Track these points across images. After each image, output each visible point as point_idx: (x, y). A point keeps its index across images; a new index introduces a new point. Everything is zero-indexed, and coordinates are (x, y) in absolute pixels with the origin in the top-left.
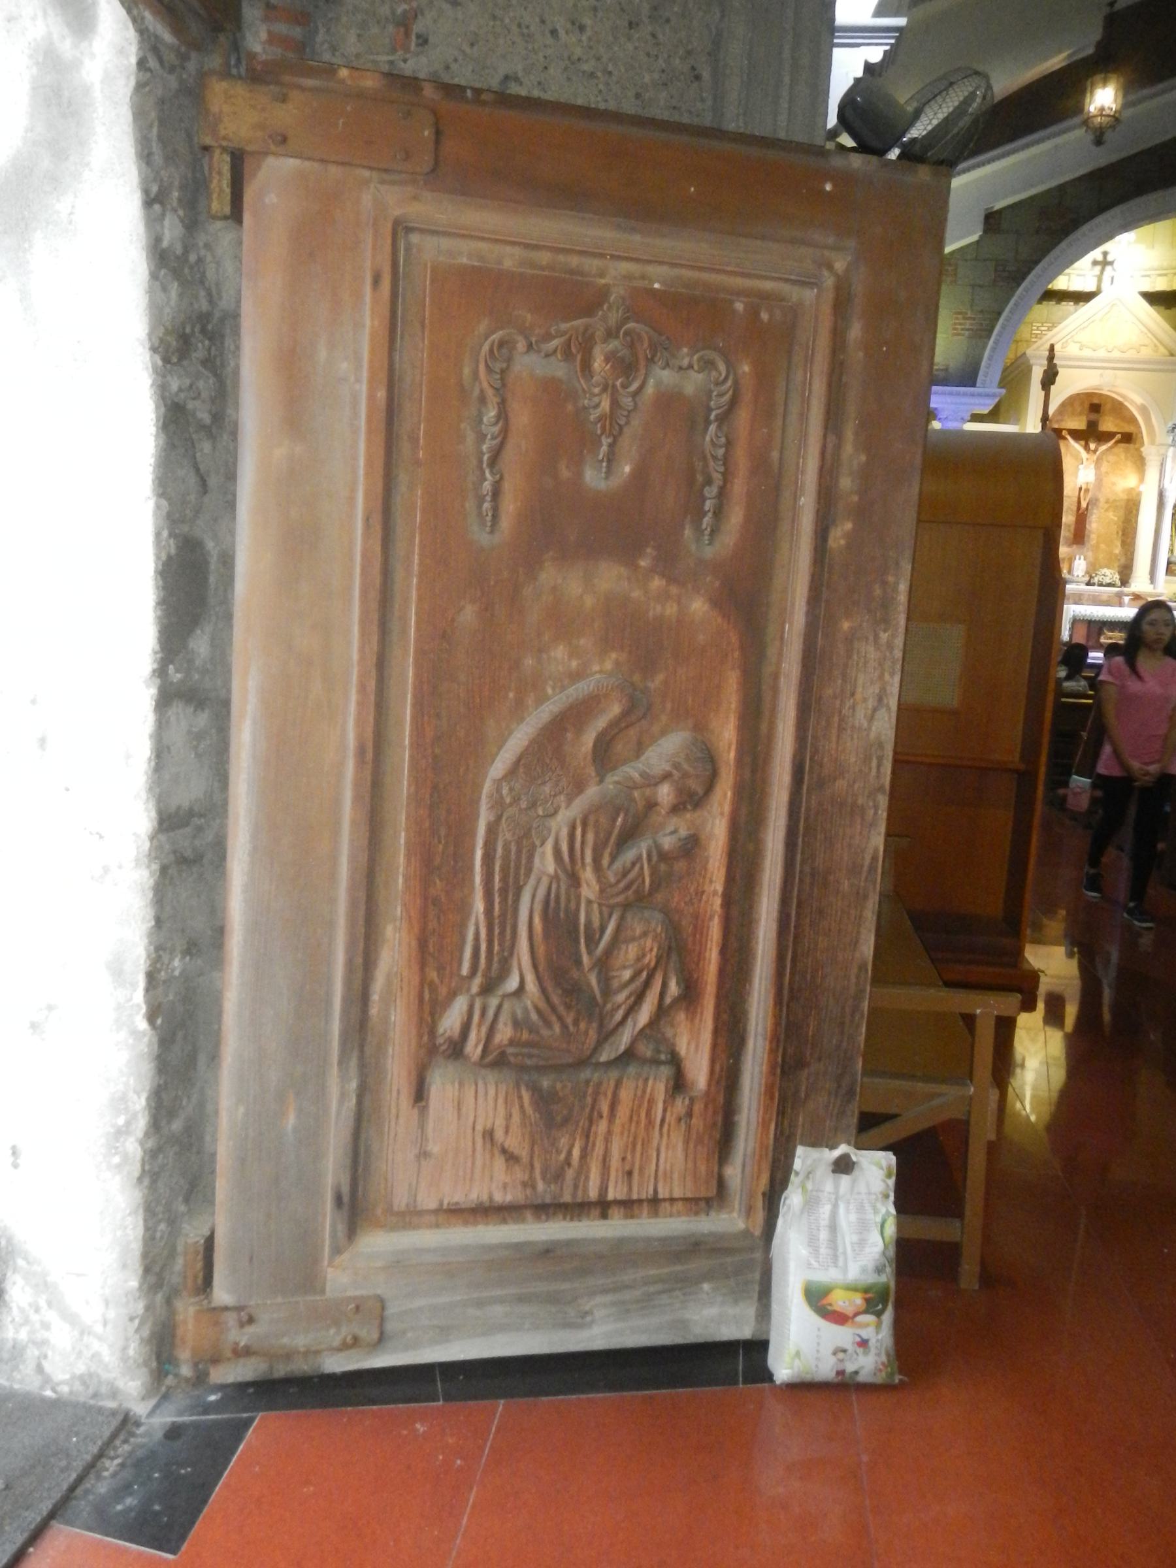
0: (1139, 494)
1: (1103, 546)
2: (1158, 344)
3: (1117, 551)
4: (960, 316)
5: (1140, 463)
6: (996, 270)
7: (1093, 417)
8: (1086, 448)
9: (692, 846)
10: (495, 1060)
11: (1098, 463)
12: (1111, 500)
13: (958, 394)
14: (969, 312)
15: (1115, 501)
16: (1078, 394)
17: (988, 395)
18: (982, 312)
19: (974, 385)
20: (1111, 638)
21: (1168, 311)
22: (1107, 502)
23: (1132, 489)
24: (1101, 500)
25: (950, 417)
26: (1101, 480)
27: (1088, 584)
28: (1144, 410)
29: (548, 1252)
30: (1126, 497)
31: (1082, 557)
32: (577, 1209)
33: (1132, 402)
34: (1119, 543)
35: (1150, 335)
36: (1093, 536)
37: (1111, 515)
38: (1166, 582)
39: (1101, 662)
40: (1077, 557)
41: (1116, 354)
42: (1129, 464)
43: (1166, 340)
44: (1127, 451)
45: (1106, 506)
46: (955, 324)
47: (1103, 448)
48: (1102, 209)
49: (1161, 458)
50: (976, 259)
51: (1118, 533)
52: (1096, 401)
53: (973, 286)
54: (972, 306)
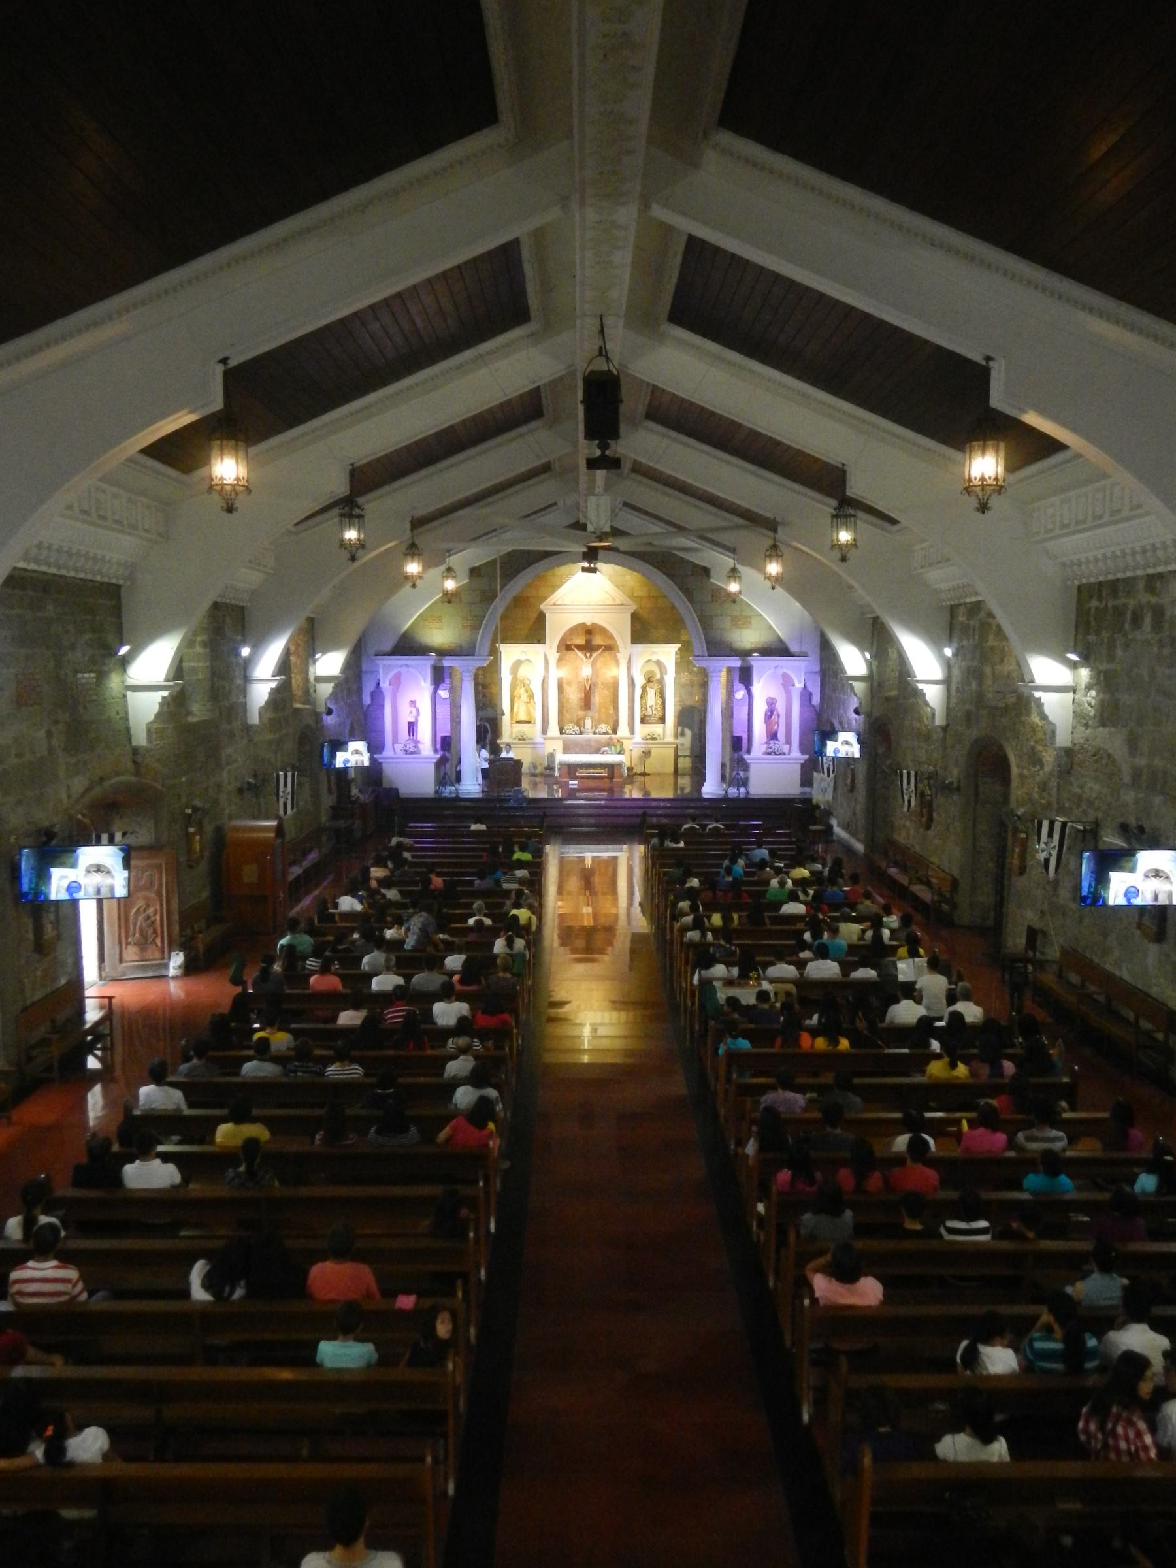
1: (603, 710)
3: (611, 711)
7: (588, 637)
8: (586, 656)
9: (155, 920)
10: (135, 944)
11: (593, 665)
13: (466, 660)
18: (476, 616)
19: (473, 655)
22: (603, 684)
27: (595, 734)
29: (143, 965)
32: (146, 960)
34: (612, 708)
37: (606, 692)
39: (576, 787)
47: (594, 655)
49: (627, 660)
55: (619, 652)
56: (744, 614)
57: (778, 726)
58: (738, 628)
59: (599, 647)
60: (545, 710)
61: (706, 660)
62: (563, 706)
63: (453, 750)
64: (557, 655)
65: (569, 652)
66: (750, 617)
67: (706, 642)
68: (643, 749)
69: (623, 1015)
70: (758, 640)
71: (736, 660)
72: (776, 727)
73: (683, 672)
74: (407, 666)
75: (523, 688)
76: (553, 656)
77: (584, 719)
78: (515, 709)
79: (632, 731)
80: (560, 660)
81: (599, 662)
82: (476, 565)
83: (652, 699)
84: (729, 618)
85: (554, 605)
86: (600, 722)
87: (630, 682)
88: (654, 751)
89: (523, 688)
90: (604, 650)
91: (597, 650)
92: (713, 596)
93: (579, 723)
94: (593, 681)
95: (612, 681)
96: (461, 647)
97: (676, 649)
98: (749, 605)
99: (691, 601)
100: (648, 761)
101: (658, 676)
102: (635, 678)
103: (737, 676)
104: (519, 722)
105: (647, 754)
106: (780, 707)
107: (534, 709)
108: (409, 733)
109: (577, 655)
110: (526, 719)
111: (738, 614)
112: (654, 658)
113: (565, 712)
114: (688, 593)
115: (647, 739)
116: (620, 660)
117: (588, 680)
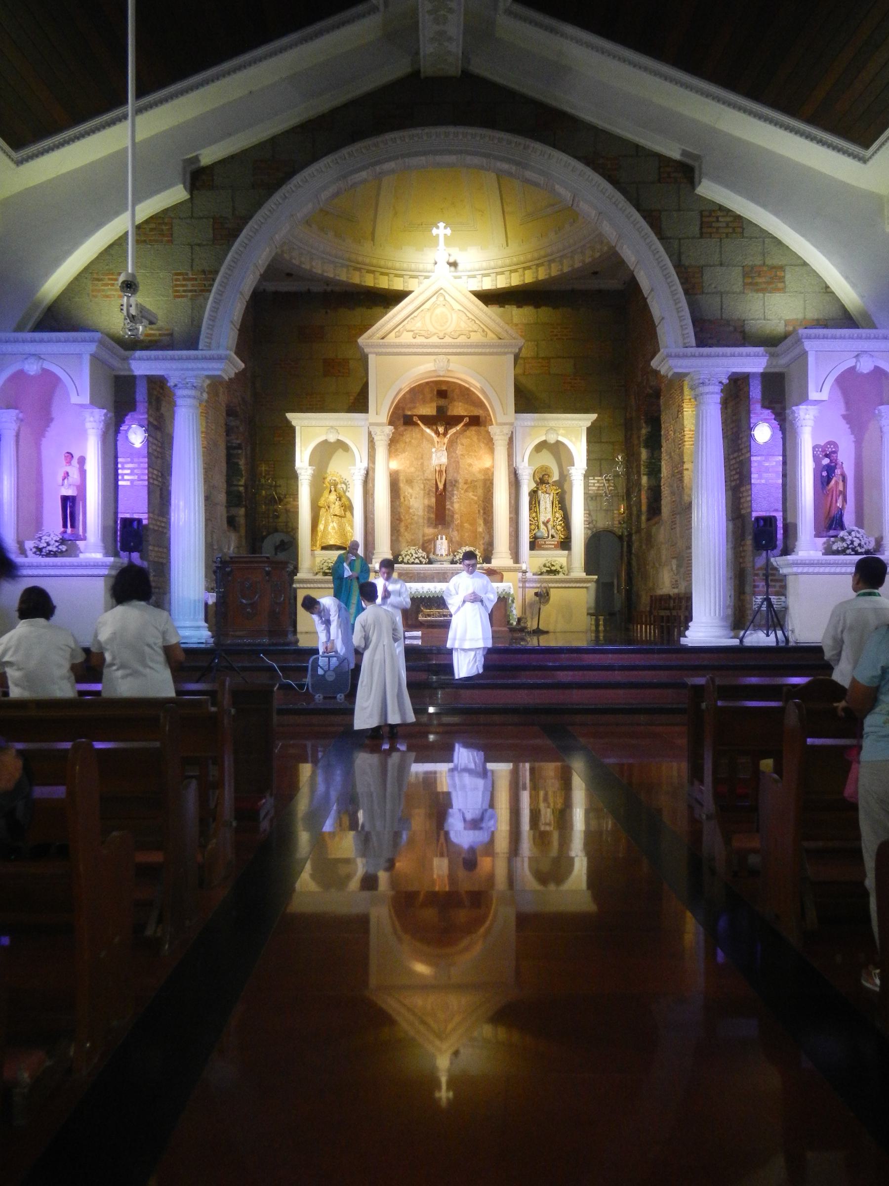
0: (493, 474)
1: (466, 525)
2: (486, 329)
3: (480, 529)
4: (180, 277)
5: (490, 443)
6: (214, 229)
7: (442, 402)
8: (437, 433)
11: (451, 447)
12: (469, 481)
13: (180, 359)
14: (190, 273)
15: (472, 481)
16: (427, 383)
17: (211, 359)
18: (204, 272)
19: (196, 349)
20: (429, 616)
21: (521, 310)
22: (466, 483)
23: (488, 469)
24: (460, 481)
25: (180, 385)
26: (458, 462)
28: (484, 393)
30: (483, 477)
31: (444, 537)
33: (476, 387)
35: (477, 322)
36: (456, 516)
37: (470, 494)
38: (531, 556)
39: (419, 642)
40: (439, 537)
41: (448, 340)
42: (482, 445)
43: (492, 325)
44: (478, 433)
45: (466, 487)
46: (177, 286)
47: (452, 431)
48: (315, 158)
49: (507, 438)
50: (192, 217)
51: (479, 511)
52: (444, 388)
53: (192, 246)
54: (192, 266)
55: (492, 424)
56: (769, 262)
57: (845, 500)
58: (758, 291)
59: (457, 420)
60: (370, 525)
61: (694, 356)
62: (400, 520)
63: (152, 550)
64: (389, 430)
65: (410, 428)
66: (782, 268)
67: (695, 322)
68: (536, 590)
69: (502, 1033)
70: (800, 316)
71: (757, 355)
72: (839, 504)
73: (594, 476)
74: (38, 357)
75: (333, 493)
76: (383, 434)
77: (433, 540)
78: (321, 527)
79: (516, 556)
80: (393, 443)
81: (459, 447)
82: (208, 156)
83: (547, 510)
84: (737, 272)
85: (383, 338)
86: (460, 545)
87: (513, 479)
88: (555, 595)
89: (333, 493)
90: (467, 425)
91: (457, 425)
92: (702, 223)
93: (428, 546)
94: (450, 478)
95: (481, 477)
96: (171, 335)
97: (589, 424)
98: (778, 243)
99: (661, 237)
100: (545, 609)
101: (556, 477)
102: (520, 472)
103: (756, 391)
104: (325, 548)
105: (543, 596)
106: (846, 459)
107: (352, 527)
108: (65, 526)
109: (422, 430)
110: (338, 543)
111: (758, 261)
112: (552, 439)
113: (402, 530)
114: (654, 219)
115: (541, 574)
116: (495, 438)
117: (440, 472)
